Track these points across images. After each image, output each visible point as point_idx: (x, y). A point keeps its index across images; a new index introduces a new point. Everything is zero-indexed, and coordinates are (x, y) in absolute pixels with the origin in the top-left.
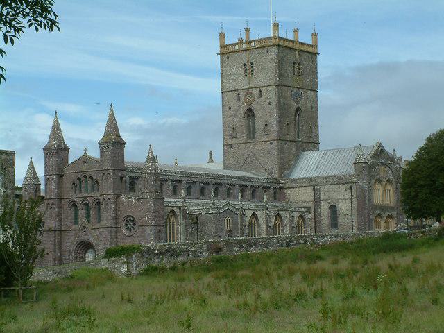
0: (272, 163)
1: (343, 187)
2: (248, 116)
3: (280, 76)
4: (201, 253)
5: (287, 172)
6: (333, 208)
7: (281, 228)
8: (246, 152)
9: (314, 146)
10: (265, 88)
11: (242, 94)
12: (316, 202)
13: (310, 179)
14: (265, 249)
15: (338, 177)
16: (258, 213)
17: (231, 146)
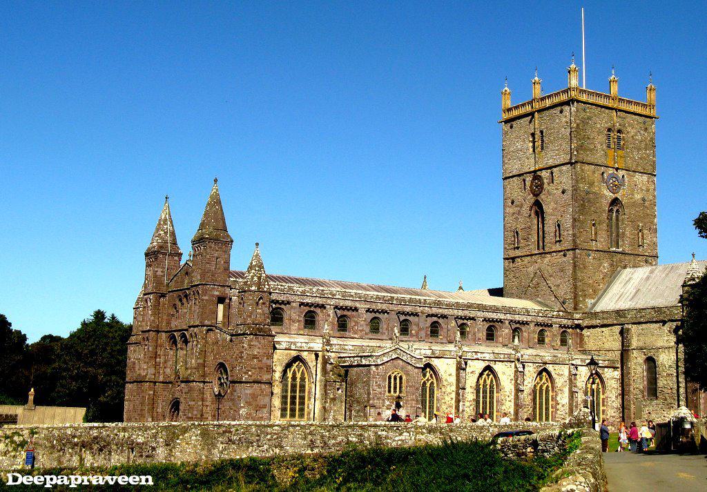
0: (565, 290)
1: (666, 328)
2: (537, 213)
3: (580, 148)
4: (154, 449)
5: (590, 302)
6: (651, 361)
7: (551, 393)
8: (531, 269)
9: (646, 261)
10: (558, 168)
11: (529, 179)
12: (625, 353)
13: (619, 313)
14: (277, 451)
15: (657, 310)
16: (498, 367)
17: (513, 259)
